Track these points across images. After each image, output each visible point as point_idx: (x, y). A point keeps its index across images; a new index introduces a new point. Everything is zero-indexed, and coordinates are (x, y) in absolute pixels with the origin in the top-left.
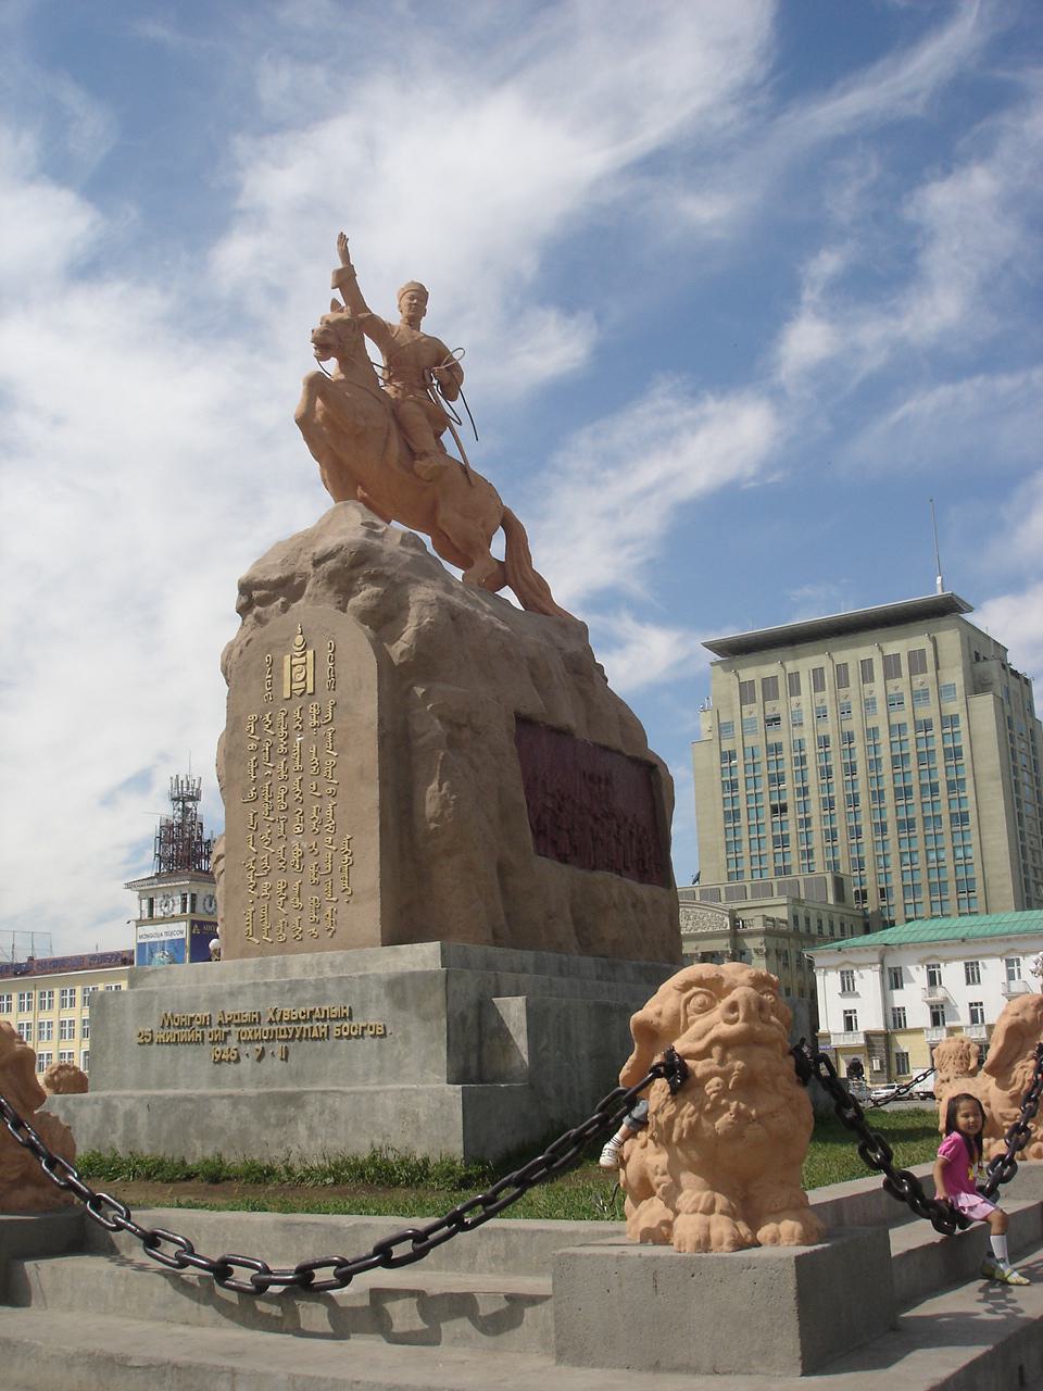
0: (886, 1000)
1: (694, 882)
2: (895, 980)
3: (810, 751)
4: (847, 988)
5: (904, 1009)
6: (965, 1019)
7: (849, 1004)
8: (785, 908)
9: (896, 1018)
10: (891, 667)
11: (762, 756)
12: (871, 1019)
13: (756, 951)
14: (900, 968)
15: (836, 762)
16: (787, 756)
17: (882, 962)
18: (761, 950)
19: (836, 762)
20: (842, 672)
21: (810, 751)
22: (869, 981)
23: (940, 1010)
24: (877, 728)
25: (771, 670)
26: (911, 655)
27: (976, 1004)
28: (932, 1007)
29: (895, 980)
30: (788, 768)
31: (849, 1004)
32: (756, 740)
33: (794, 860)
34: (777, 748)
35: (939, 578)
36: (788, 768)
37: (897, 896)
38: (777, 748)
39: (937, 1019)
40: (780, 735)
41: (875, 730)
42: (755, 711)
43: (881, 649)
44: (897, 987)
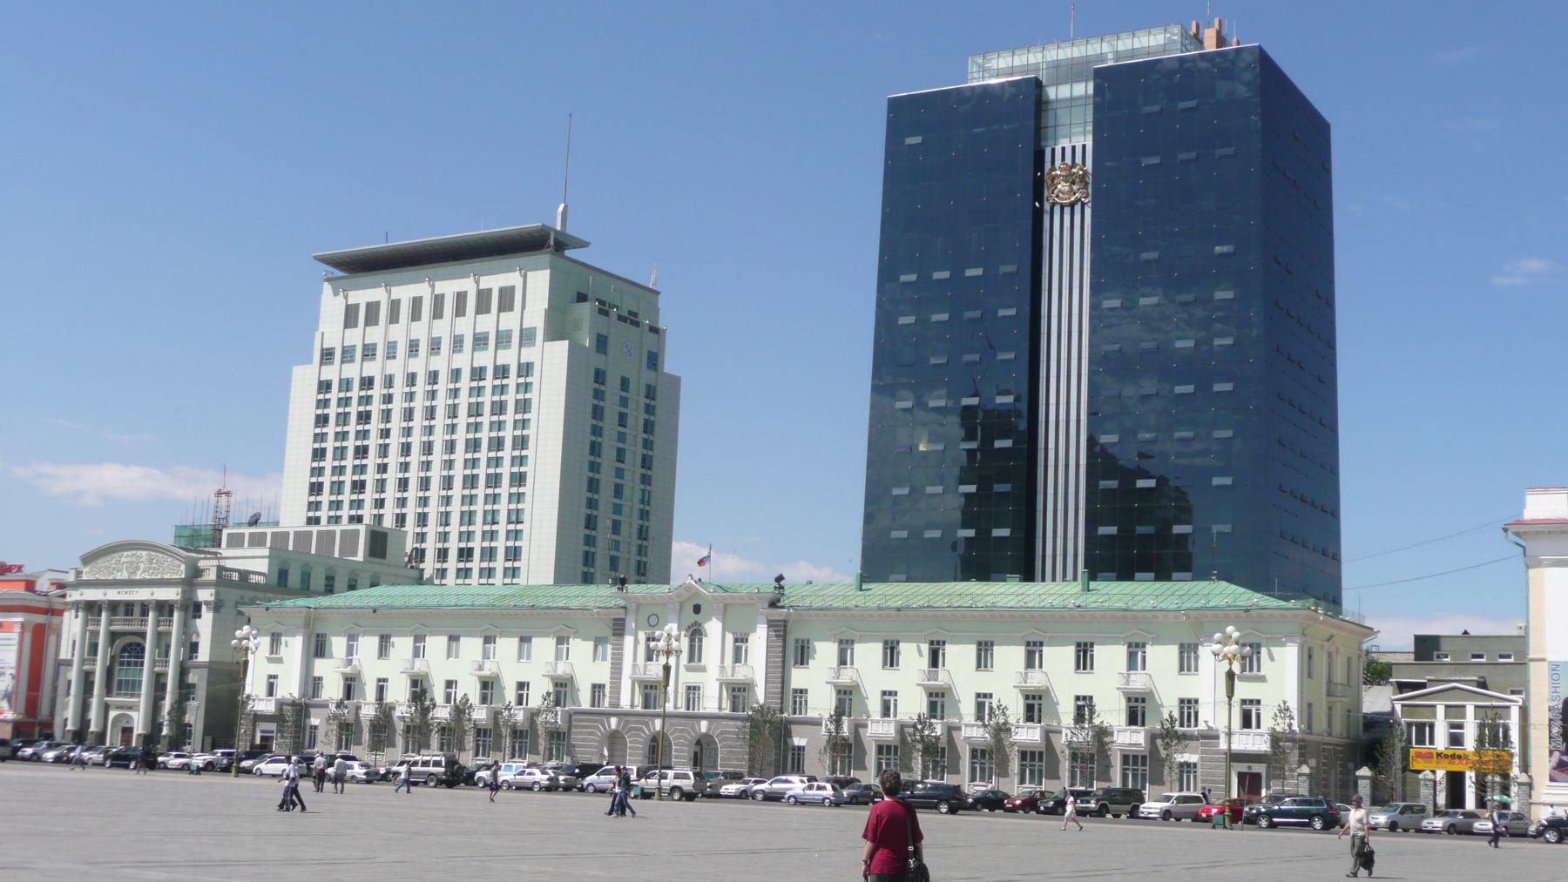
0: (307, 667)
2: (318, 648)
3: (398, 390)
4: (274, 657)
7: (273, 669)
9: (312, 684)
12: (290, 688)
13: (207, 603)
16: (377, 392)
17: (307, 625)
21: (398, 390)
22: (294, 646)
23: (353, 683)
24: (533, 363)
26: (502, 291)
29: (318, 648)
31: (273, 669)
33: (368, 512)
42: (355, 337)
43: (477, 283)
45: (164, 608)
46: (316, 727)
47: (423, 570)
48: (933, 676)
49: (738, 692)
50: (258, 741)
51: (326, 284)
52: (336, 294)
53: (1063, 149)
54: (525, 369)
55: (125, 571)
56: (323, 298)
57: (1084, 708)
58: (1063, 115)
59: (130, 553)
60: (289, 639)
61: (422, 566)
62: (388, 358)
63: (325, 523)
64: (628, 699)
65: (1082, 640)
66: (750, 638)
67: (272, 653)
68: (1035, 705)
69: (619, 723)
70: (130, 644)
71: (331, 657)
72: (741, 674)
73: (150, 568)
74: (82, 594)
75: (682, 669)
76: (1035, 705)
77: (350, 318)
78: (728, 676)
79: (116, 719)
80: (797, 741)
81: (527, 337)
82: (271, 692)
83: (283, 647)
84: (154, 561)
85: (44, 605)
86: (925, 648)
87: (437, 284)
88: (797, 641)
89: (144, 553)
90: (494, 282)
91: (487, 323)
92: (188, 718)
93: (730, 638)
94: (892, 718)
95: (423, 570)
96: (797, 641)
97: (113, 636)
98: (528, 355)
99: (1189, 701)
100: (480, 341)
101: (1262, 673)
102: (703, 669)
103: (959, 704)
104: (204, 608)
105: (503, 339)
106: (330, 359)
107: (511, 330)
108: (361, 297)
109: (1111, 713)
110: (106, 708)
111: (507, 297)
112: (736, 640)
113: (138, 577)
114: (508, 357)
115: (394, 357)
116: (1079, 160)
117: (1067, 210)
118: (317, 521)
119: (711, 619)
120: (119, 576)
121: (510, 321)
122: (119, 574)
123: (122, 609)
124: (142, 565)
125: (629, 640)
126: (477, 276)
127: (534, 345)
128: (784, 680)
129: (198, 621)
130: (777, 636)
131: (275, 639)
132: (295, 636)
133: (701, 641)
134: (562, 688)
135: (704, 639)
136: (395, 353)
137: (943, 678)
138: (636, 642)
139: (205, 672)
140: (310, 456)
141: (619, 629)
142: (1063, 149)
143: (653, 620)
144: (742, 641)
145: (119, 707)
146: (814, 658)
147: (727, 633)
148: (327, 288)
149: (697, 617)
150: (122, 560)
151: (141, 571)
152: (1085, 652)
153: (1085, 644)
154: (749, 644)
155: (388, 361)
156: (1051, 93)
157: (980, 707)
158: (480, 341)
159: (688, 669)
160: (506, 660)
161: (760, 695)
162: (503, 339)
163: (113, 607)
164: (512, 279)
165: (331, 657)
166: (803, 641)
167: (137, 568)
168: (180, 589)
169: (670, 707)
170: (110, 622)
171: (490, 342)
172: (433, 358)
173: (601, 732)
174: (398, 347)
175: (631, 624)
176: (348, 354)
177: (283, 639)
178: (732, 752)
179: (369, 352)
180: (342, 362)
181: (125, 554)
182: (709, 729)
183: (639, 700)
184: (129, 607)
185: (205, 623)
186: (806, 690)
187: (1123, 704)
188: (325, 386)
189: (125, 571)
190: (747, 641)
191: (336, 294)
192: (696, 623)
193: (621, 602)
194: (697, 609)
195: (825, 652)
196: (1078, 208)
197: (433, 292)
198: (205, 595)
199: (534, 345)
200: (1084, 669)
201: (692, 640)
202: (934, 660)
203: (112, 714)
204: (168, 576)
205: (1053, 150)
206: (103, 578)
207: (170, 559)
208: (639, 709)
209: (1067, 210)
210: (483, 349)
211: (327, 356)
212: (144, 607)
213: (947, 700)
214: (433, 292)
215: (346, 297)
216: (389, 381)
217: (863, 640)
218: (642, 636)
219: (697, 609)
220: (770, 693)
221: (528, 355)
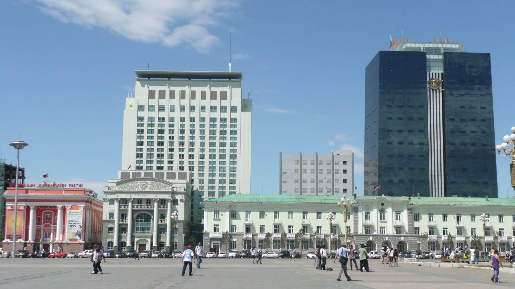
0: (230, 222)
1: (129, 168)
2: (234, 216)
5: (236, 225)
6: (441, 233)
7: (216, 223)
8: (186, 184)
9: (233, 228)
10: (213, 95)
11: (156, 122)
12: (224, 228)
13: (181, 200)
14: (236, 211)
15: (187, 129)
16: (167, 123)
17: (230, 208)
18: (183, 200)
19: (187, 129)
20: (193, 95)
22: (225, 216)
23: (249, 227)
25: (165, 88)
26: (222, 93)
27: (216, 225)
28: (246, 226)
29: (234, 216)
30: (166, 128)
31: (216, 223)
32: (155, 114)
33: (166, 165)
34: (163, 119)
35: (230, 65)
36: (166, 128)
37: (206, 184)
38: (163, 119)
39: (248, 230)
40: (163, 114)
41: (204, 118)
42: (156, 102)
44: (234, 218)
45: (163, 202)
46: (235, 242)
47: (193, 186)
48: (458, 223)
49: (398, 229)
50: (212, 247)
51: (137, 82)
52: (143, 86)
53: (433, 73)
54: (233, 120)
55: (139, 188)
56: (136, 86)
57: (473, 230)
58: (432, 64)
59: (142, 181)
60: (223, 213)
61: (192, 185)
62: (171, 111)
63: (146, 169)
64: (361, 231)
65: (500, 214)
66: (401, 213)
67: (214, 217)
68: (460, 231)
69: (373, 238)
70: (141, 214)
71: (240, 219)
72: (399, 223)
73: (153, 187)
74: (118, 196)
75: (379, 222)
76: (460, 231)
77: (151, 94)
78: (395, 224)
79: (138, 241)
80: (234, 240)
81: (234, 109)
82: (215, 230)
83: (220, 215)
84: (155, 185)
85: (86, 199)
86: (456, 216)
87: (191, 87)
88: (415, 214)
89: (149, 182)
90: (219, 90)
91: (217, 103)
92: (176, 240)
93: (394, 213)
94: (217, 232)
95: (193, 186)
96: (415, 214)
97: (134, 211)
98: (234, 115)
99: (383, 227)
100: (213, 109)
101: (386, 220)
102: (386, 222)
103: (467, 232)
104: (179, 202)
105: (223, 109)
106: (143, 109)
107: (216, 106)
108: (157, 89)
109: (453, 232)
110: (133, 237)
111: (224, 96)
112: (396, 214)
113: (147, 190)
114: (227, 115)
115: (174, 111)
116: (437, 77)
117: (434, 91)
118: (141, 168)
119: (388, 208)
120: (137, 189)
121: (224, 103)
122: (137, 189)
123: (136, 202)
124: (149, 186)
125: (360, 214)
126: (211, 86)
127: (237, 112)
128: (413, 224)
129: (177, 206)
130: (411, 212)
131: (216, 213)
132: (226, 212)
133: (384, 213)
134: (334, 228)
135: (385, 213)
136: (174, 109)
137: (461, 224)
138: (362, 214)
139: (182, 224)
140: (136, 144)
141: (355, 210)
142: (433, 73)
143: (367, 207)
144: (398, 214)
145: (139, 237)
146: (421, 220)
147: (393, 212)
148: (138, 84)
149: (383, 207)
150: (138, 184)
151: (149, 188)
152: (501, 217)
153: (501, 215)
154: (401, 215)
155: (171, 112)
156: (428, 56)
157: (472, 232)
158: (213, 109)
159: (381, 222)
160: (284, 219)
161: (407, 229)
162: (223, 109)
163: (133, 201)
164: (227, 89)
165: (240, 219)
166: (417, 214)
167: (147, 187)
168: (183, 196)
169: (375, 233)
170: (133, 206)
171: (227, 110)
172: (192, 113)
173: (366, 241)
174: (196, 108)
175: (360, 208)
176: (151, 108)
177: (220, 213)
178: (412, 246)
179: (162, 108)
180: (148, 111)
181: (139, 182)
182: (404, 240)
183: (364, 231)
184: (139, 201)
185: (181, 207)
186: (321, 227)
187: (456, 230)
188: (141, 119)
189: (139, 188)
190: (400, 214)
191: (143, 86)
192: (383, 208)
193: (356, 202)
194: (383, 204)
195: (425, 217)
196: (438, 90)
197: (190, 90)
198: (178, 197)
199: (226, 112)
200: (501, 221)
201: (381, 213)
202: (458, 220)
203: (136, 240)
204: (163, 190)
205: (430, 73)
206: (128, 190)
207: (163, 184)
208: (364, 234)
209: (434, 91)
210: (214, 112)
211: (141, 108)
212: (149, 202)
213: (462, 230)
214: (190, 90)
215: (149, 87)
216: (172, 119)
217: (437, 214)
218: (364, 212)
219: (383, 204)
220: (409, 229)
221: (234, 115)
